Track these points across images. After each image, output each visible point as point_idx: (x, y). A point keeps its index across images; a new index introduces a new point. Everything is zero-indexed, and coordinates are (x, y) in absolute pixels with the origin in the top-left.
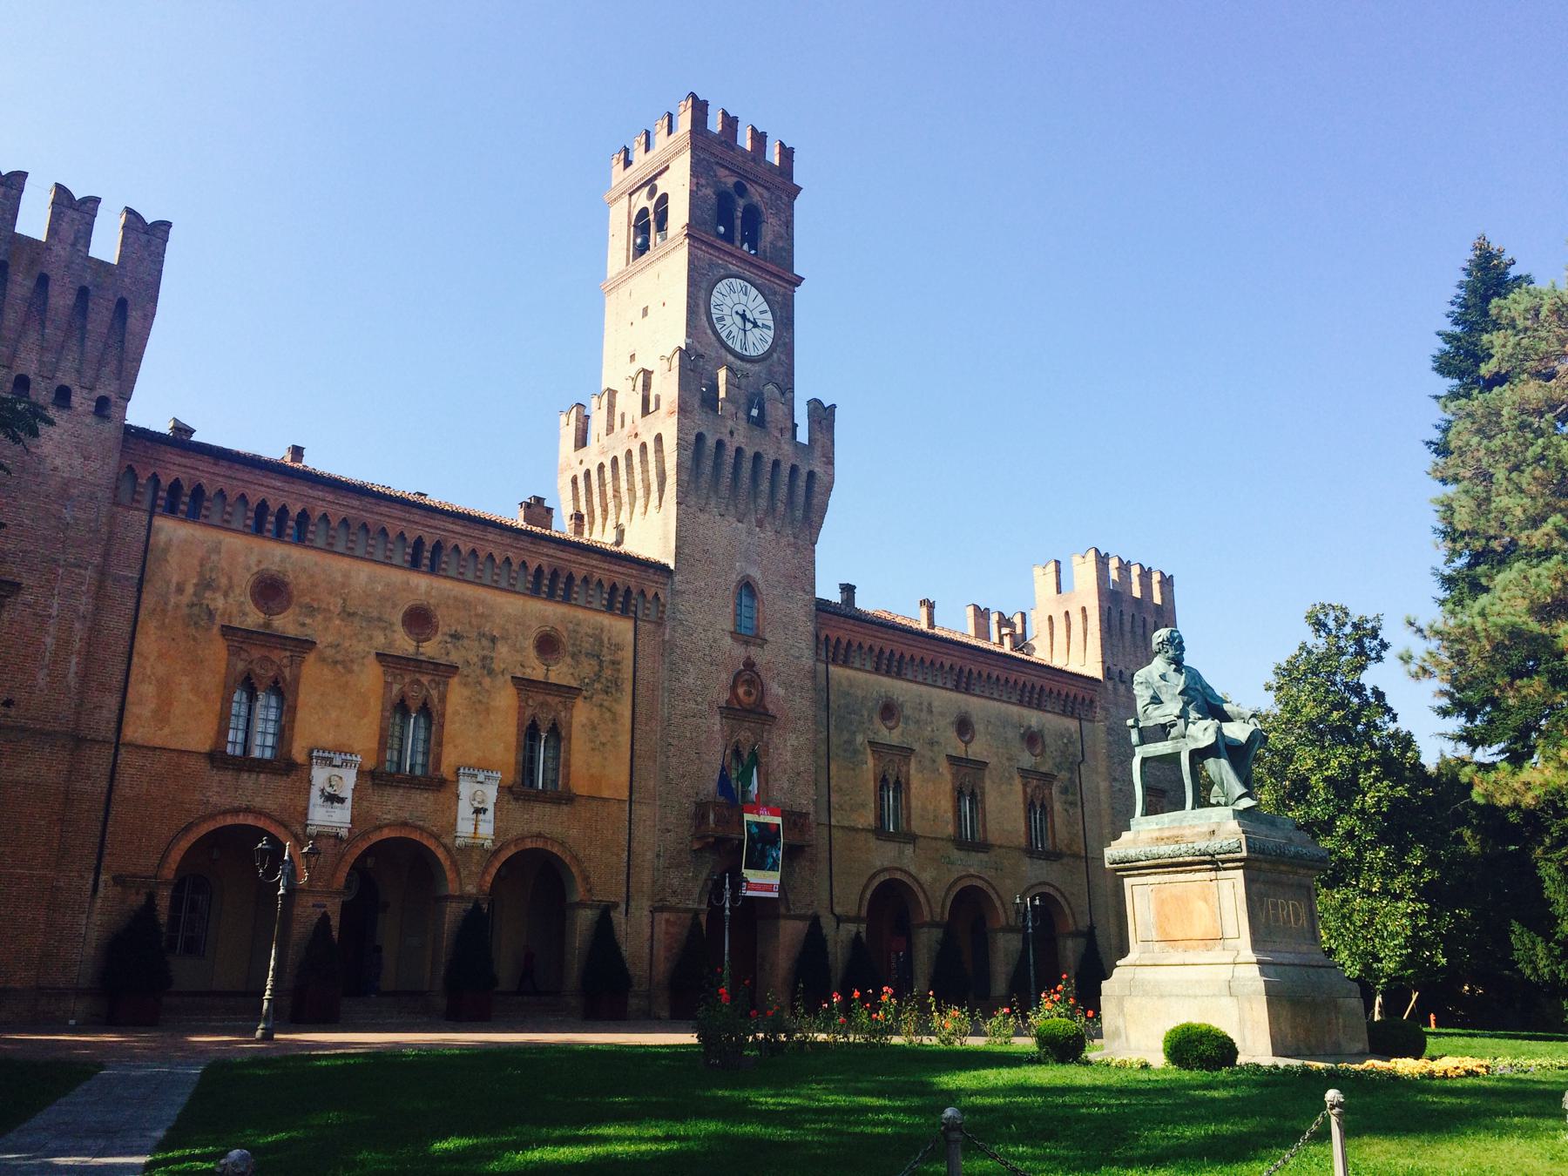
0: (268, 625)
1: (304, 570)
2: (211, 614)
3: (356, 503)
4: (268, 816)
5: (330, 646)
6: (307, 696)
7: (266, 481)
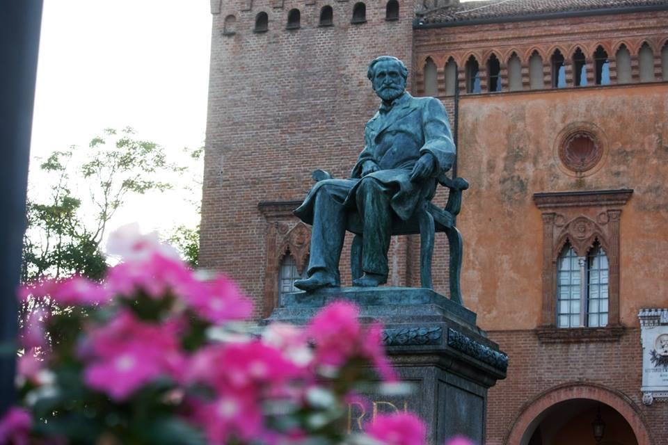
0: (580, 183)
1: (612, 113)
2: (522, 186)
3: (652, 22)
4: (602, 388)
5: (649, 190)
6: (630, 251)
7: (554, 29)
